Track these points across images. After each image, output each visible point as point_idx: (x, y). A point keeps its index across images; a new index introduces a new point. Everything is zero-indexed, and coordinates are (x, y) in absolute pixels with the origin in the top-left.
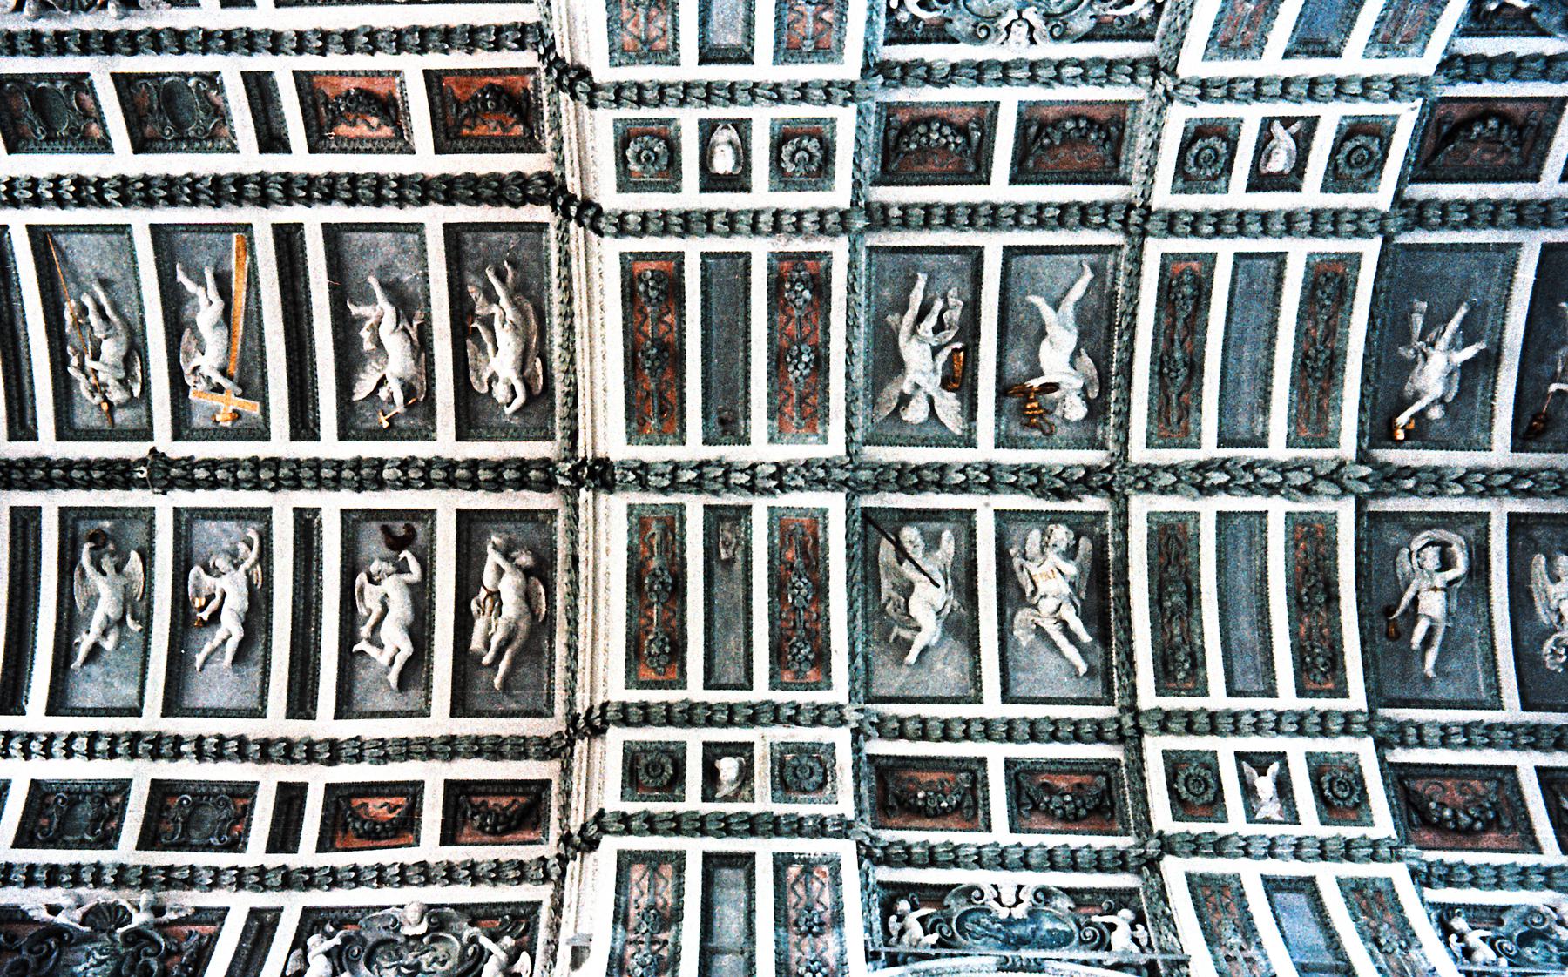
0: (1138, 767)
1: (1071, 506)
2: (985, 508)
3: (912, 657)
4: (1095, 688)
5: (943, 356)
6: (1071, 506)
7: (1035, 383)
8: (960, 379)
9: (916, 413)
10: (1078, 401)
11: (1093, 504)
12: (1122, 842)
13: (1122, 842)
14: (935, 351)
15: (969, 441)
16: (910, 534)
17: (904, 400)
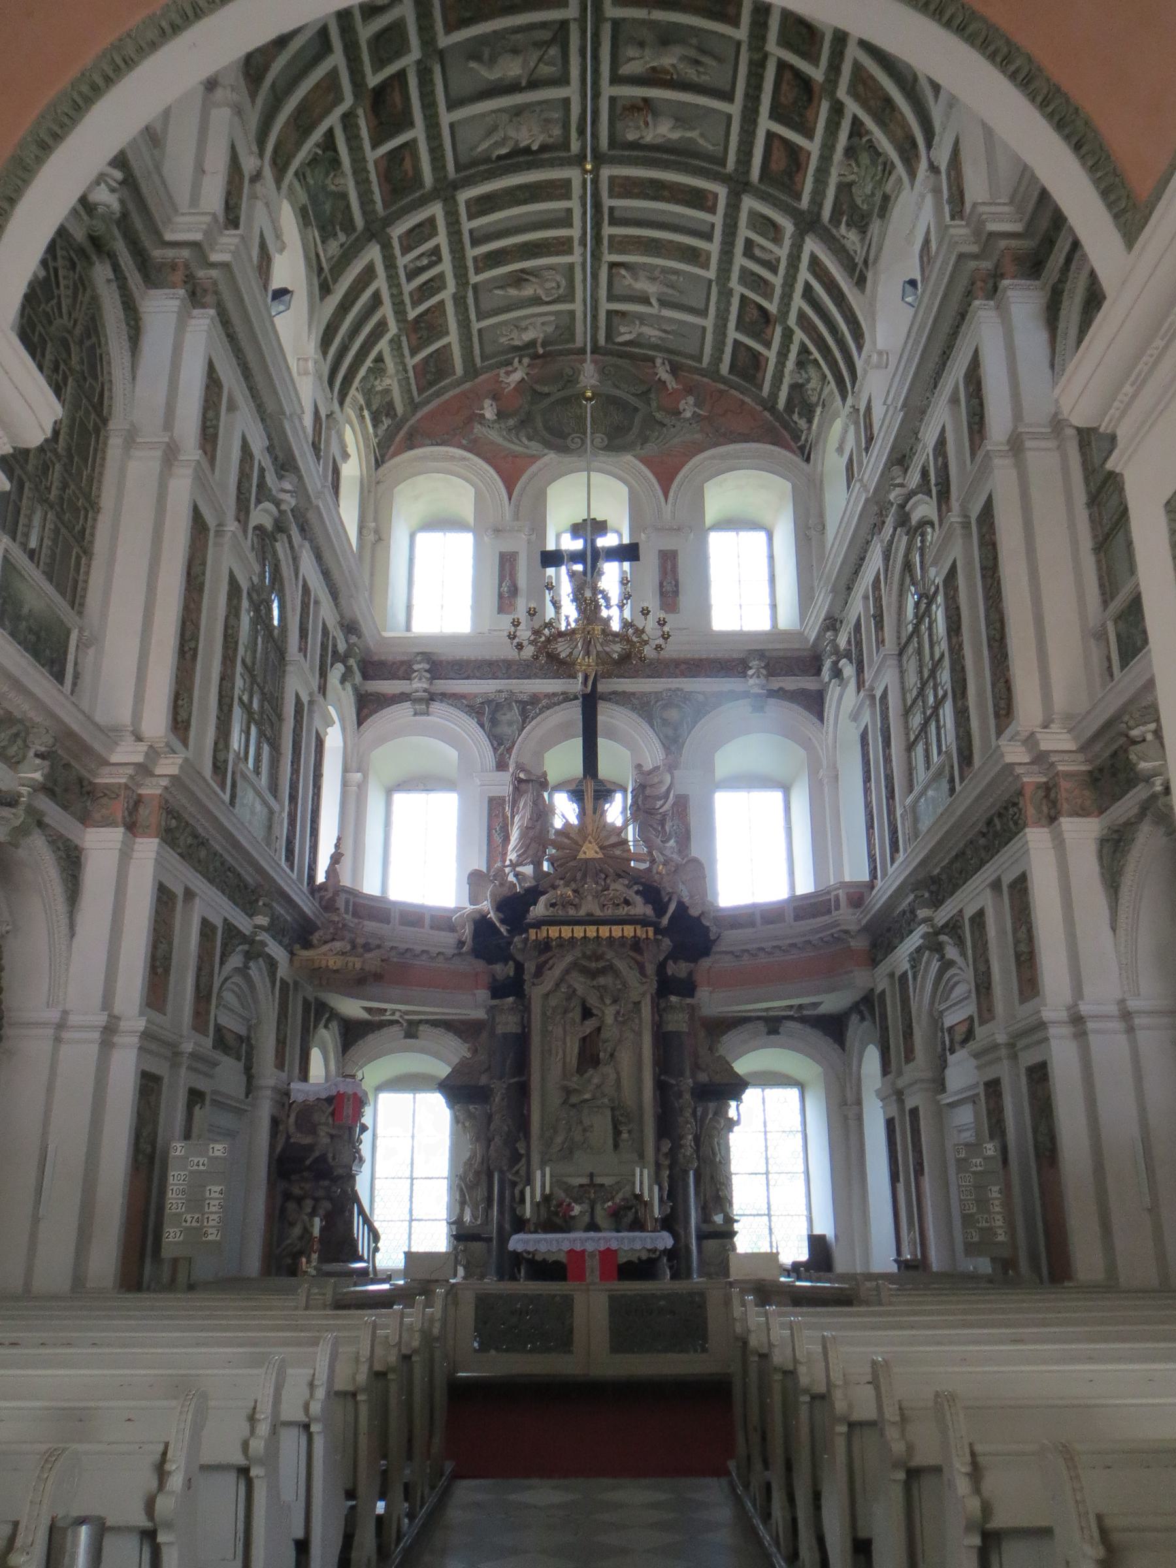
0: (423, 201)
1: (574, 134)
2: (571, 91)
3: (473, 65)
4: (463, 159)
5: (671, 70)
6: (574, 134)
7: (649, 119)
8: (654, 78)
9: (631, 52)
10: (637, 137)
11: (575, 146)
12: (379, 206)
13: (379, 206)
14: (673, 66)
15: (616, 79)
16: (553, 51)
17: (642, 45)
